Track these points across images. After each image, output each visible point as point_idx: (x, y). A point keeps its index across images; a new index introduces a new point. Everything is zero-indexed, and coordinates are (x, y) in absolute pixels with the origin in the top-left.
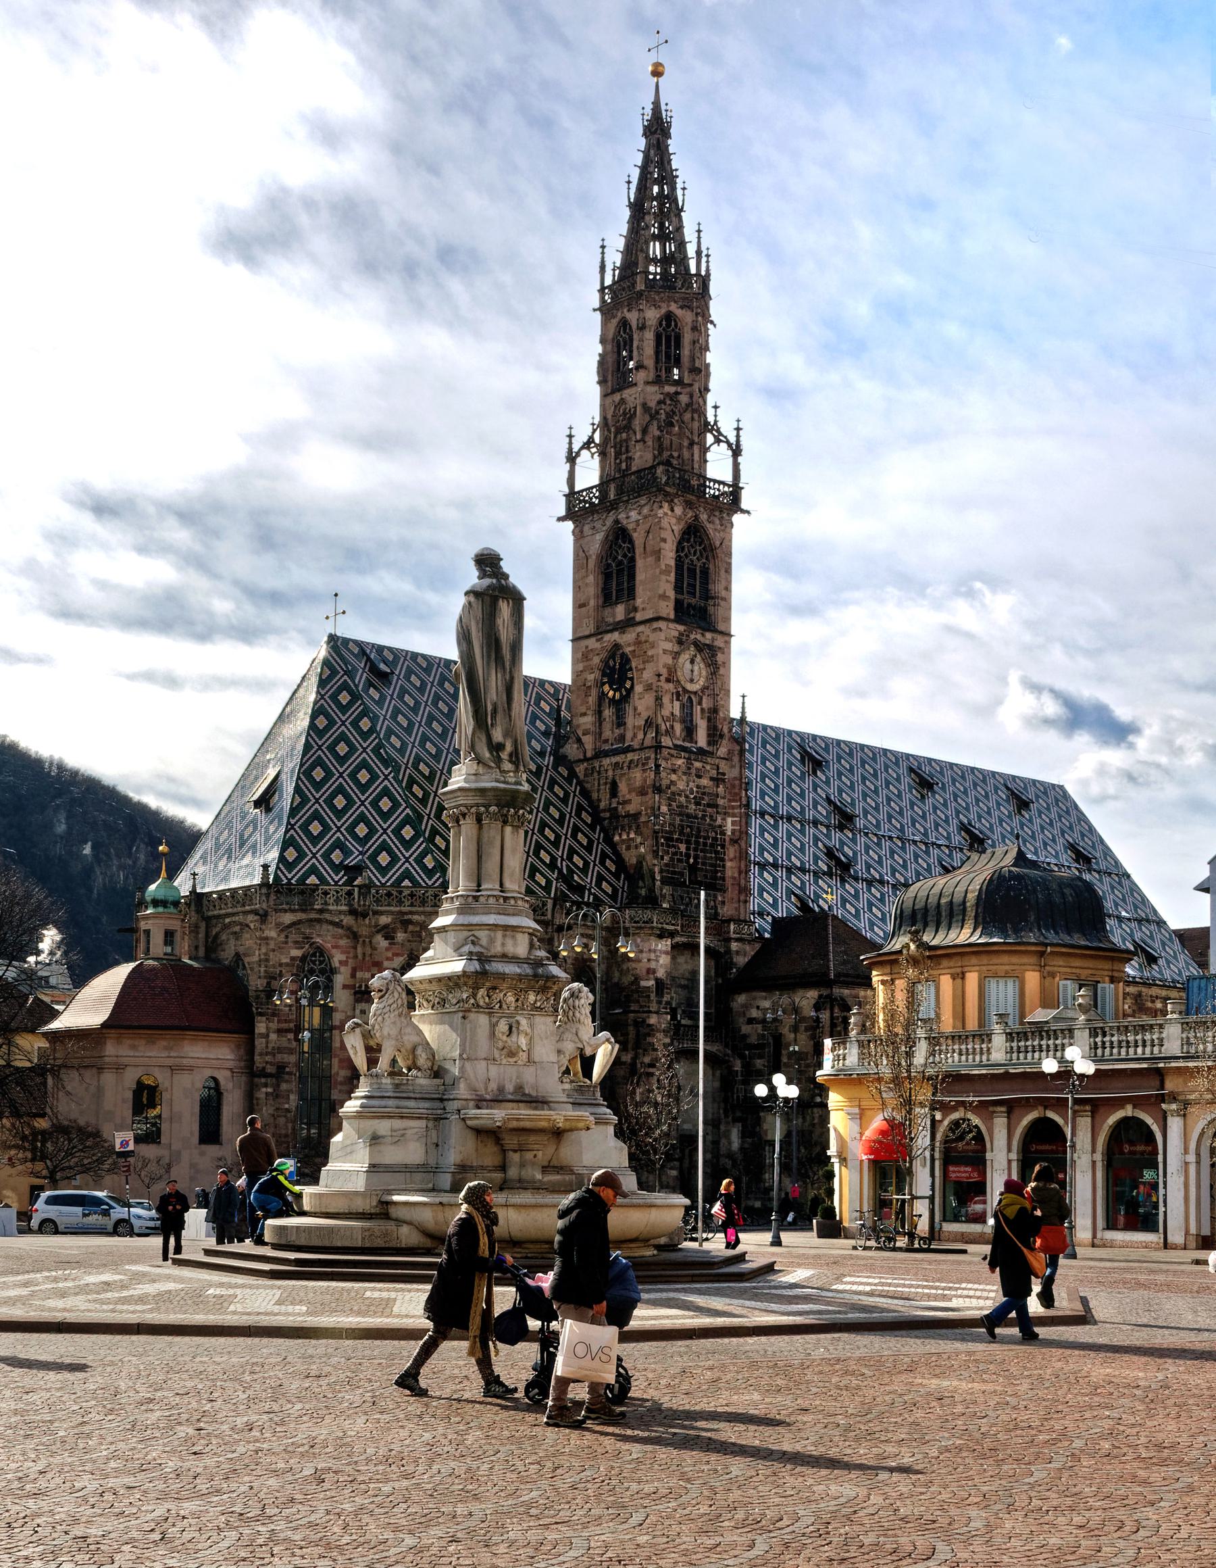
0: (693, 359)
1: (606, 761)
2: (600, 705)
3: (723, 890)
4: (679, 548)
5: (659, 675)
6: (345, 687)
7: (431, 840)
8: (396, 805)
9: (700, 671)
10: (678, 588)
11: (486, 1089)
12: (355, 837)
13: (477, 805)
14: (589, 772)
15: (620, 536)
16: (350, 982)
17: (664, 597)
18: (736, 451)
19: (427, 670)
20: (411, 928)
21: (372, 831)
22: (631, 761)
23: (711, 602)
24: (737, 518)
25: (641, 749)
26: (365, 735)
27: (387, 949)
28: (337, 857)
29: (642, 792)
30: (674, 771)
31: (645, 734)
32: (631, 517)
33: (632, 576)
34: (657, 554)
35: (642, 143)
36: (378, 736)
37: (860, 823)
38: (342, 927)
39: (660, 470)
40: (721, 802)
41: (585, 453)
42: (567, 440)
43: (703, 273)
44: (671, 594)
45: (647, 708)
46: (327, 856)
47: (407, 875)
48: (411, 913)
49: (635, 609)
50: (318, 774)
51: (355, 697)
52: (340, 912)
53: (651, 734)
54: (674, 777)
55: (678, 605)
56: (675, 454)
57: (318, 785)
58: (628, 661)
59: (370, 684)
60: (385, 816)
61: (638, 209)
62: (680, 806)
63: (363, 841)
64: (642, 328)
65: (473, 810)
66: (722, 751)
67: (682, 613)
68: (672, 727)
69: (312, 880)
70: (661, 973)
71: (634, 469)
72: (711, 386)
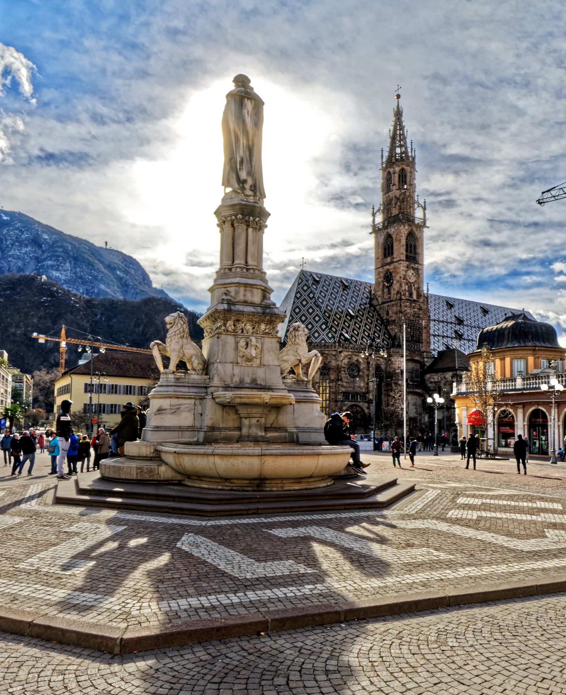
0: (410, 181)
1: (385, 305)
3: (422, 343)
4: (407, 239)
6: (306, 285)
7: (331, 329)
8: (320, 319)
10: (407, 251)
14: (380, 308)
17: (402, 254)
19: (331, 280)
26: (311, 299)
29: (396, 313)
32: (392, 230)
34: (400, 241)
35: (394, 119)
39: (400, 215)
44: (404, 252)
47: (323, 339)
50: (297, 310)
51: (309, 287)
55: (407, 256)
57: (297, 314)
59: (313, 284)
60: (317, 322)
61: (393, 138)
64: (394, 173)
66: (421, 300)
67: (408, 258)
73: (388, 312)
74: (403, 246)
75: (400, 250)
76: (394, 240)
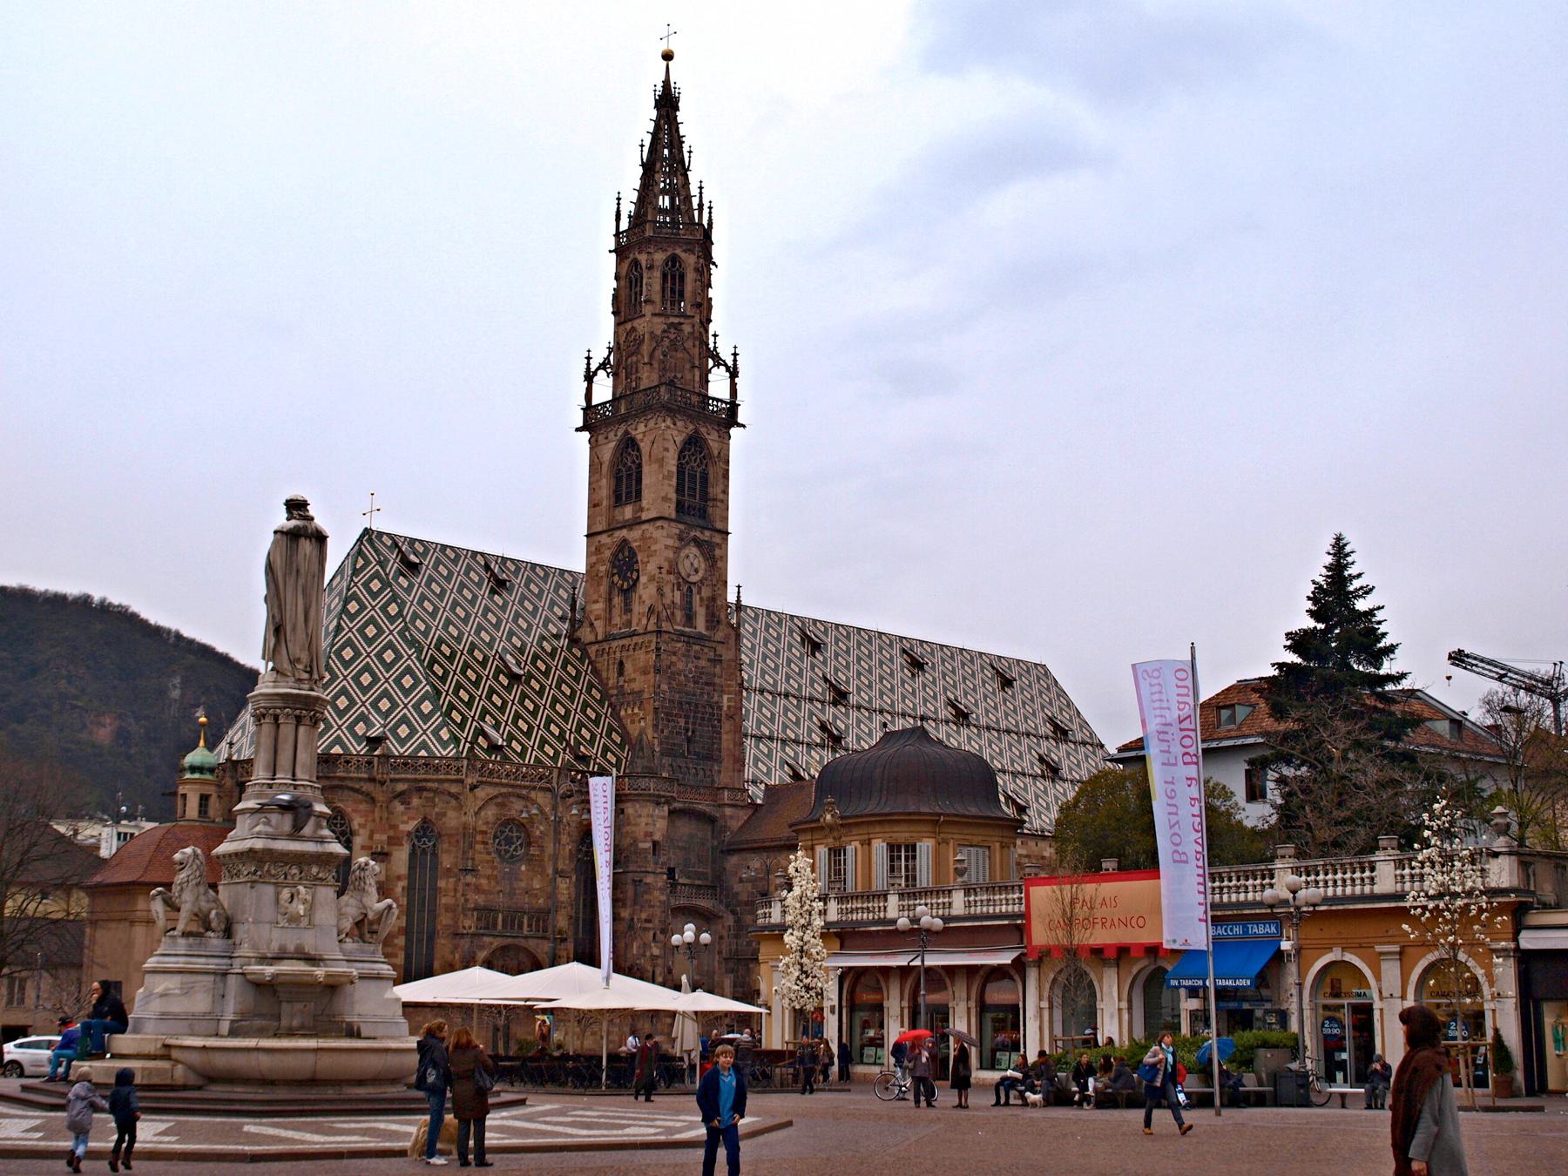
1: (615, 644)
2: (610, 593)
3: (719, 761)
4: (681, 456)
5: (660, 568)
6: (376, 575)
7: (448, 714)
8: (417, 682)
9: (700, 563)
10: (680, 489)
11: (268, 948)
12: (378, 710)
13: (275, 708)
15: (629, 444)
16: (368, 843)
18: (733, 373)
20: (425, 794)
21: (394, 705)
22: (636, 644)
23: (710, 503)
24: (734, 431)
25: (645, 634)
26: (392, 619)
27: (403, 814)
28: (361, 729)
30: (674, 654)
31: (648, 620)
32: (639, 430)
33: (639, 481)
34: (661, 462)
35: (654, 114)
36: (404, 620)
37: (853, 699)
38: (362, 793)
39: (663, 389)
40: (717, 680)
41: (601, 373)
42: (586, 361)
43: (705, 222)
44: (673, 496)
45: (650, 597)
46: (351, 728)
48: (426, 780)
49: (641, 509)
51: (386, 584)
52: (361, 779)
53: (653, 620)
54: (674, 659)
55: (680, 507)
56: (679, 376)
58: (635, 554)
60: (407, 692)
61: (649, 168)
62: (680, 684)
63: (386, 715)
64: (650, 268)
65: (271, 711)
66: (719, 636)
68: (673, 613)
69: (337, 750)
70: (657, 837)
71: (642, 388)
72: (713, 317)
73: (621, 664)
74: (668, 477)
75: (658, 488)
76: (645, 458)
